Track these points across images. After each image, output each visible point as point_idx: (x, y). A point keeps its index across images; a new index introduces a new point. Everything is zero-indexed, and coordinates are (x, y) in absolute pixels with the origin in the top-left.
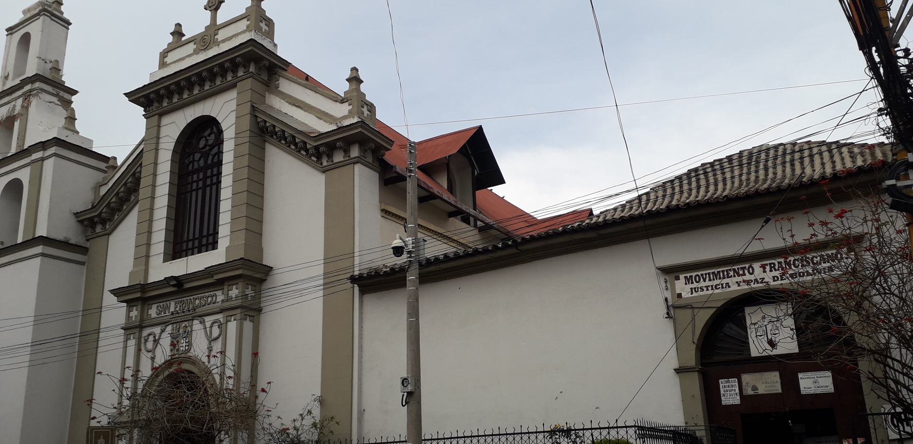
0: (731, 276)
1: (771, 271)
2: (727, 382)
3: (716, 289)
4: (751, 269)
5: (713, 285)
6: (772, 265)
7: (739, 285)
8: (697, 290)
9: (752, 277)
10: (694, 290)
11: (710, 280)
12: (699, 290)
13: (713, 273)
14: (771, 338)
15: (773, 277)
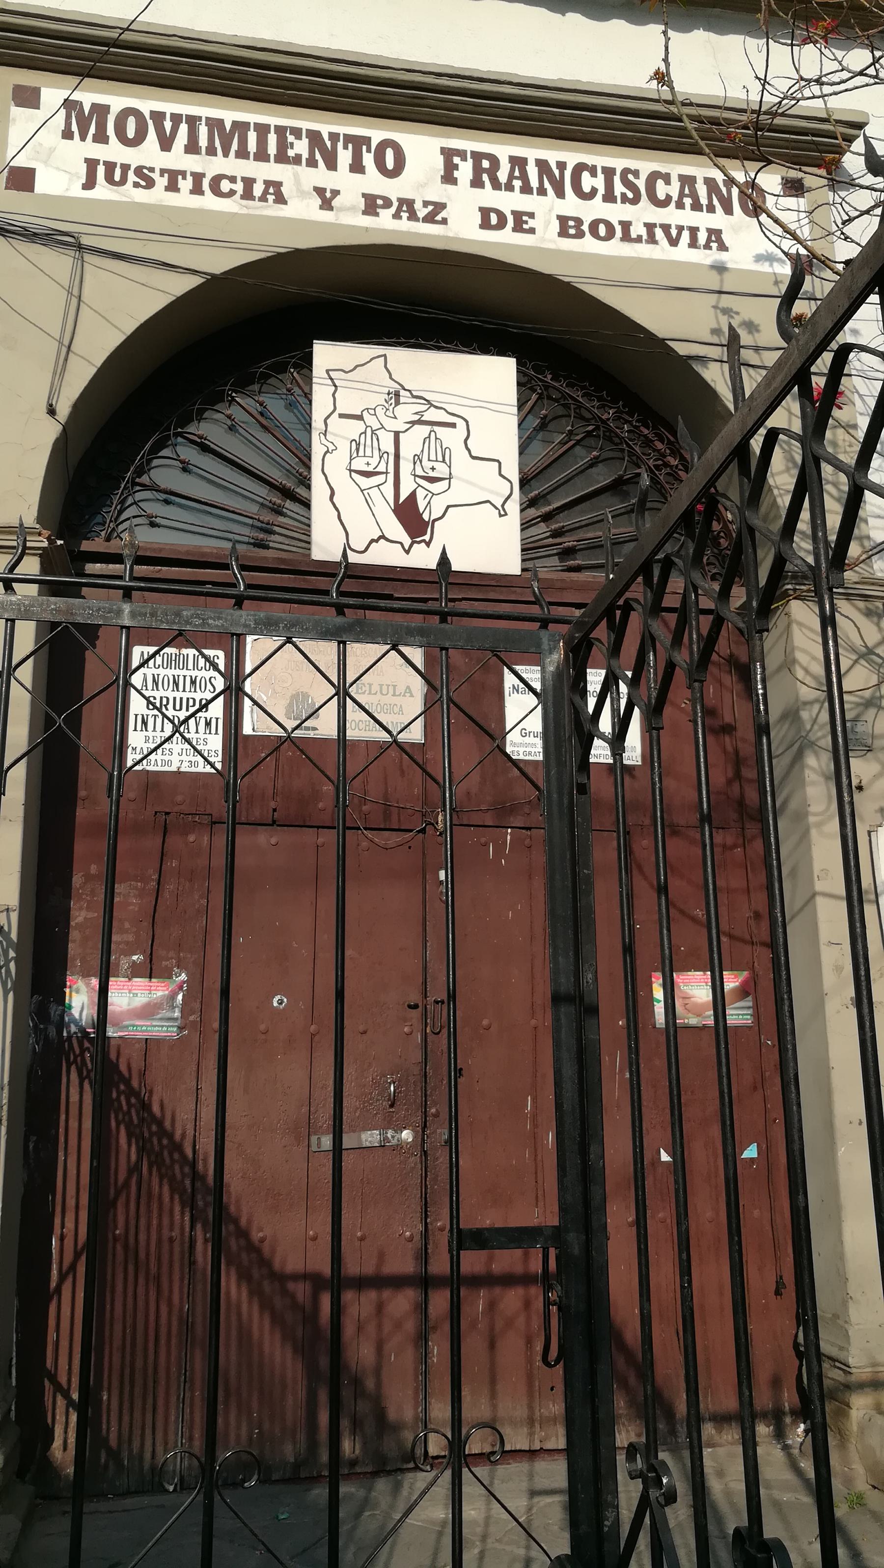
0: (297, 160)
1: (476, 183)
2: (170, 662)
3: (216, 190)
4: (390, 155)
5: (203, 175)
6: (486, 164)
7: (327, 205)
8: (117, 178)
9: (393, 189)
10: (101, 170)
11: (192, 148)
12: (132, 177)
13: (215, 124)
14: (413, 496)
15: (481, 209)
